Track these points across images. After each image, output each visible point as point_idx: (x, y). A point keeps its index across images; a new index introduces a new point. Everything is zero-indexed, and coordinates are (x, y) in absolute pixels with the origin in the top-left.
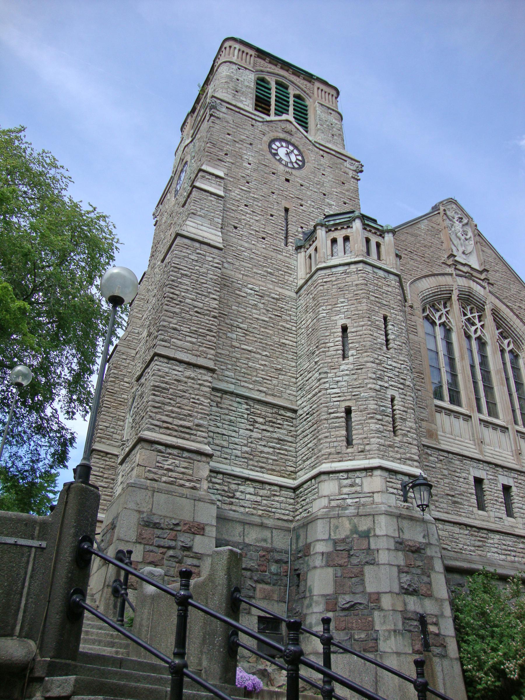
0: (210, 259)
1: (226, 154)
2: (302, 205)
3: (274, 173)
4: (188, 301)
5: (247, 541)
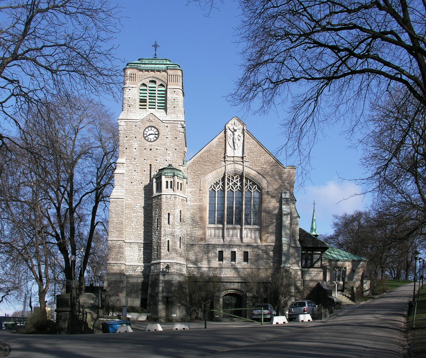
0: (121, 204)
1: (126, 149)
2: (156, 160)
3: (145, 149)
4: (115, 221)
5: (138, 281)
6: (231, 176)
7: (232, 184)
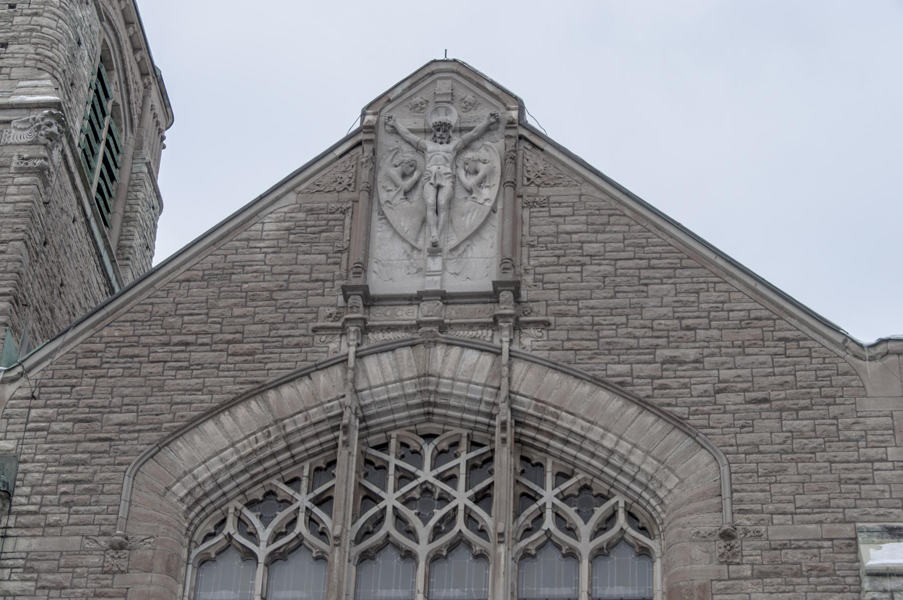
6: (393, 444)
7: (407, 501)
